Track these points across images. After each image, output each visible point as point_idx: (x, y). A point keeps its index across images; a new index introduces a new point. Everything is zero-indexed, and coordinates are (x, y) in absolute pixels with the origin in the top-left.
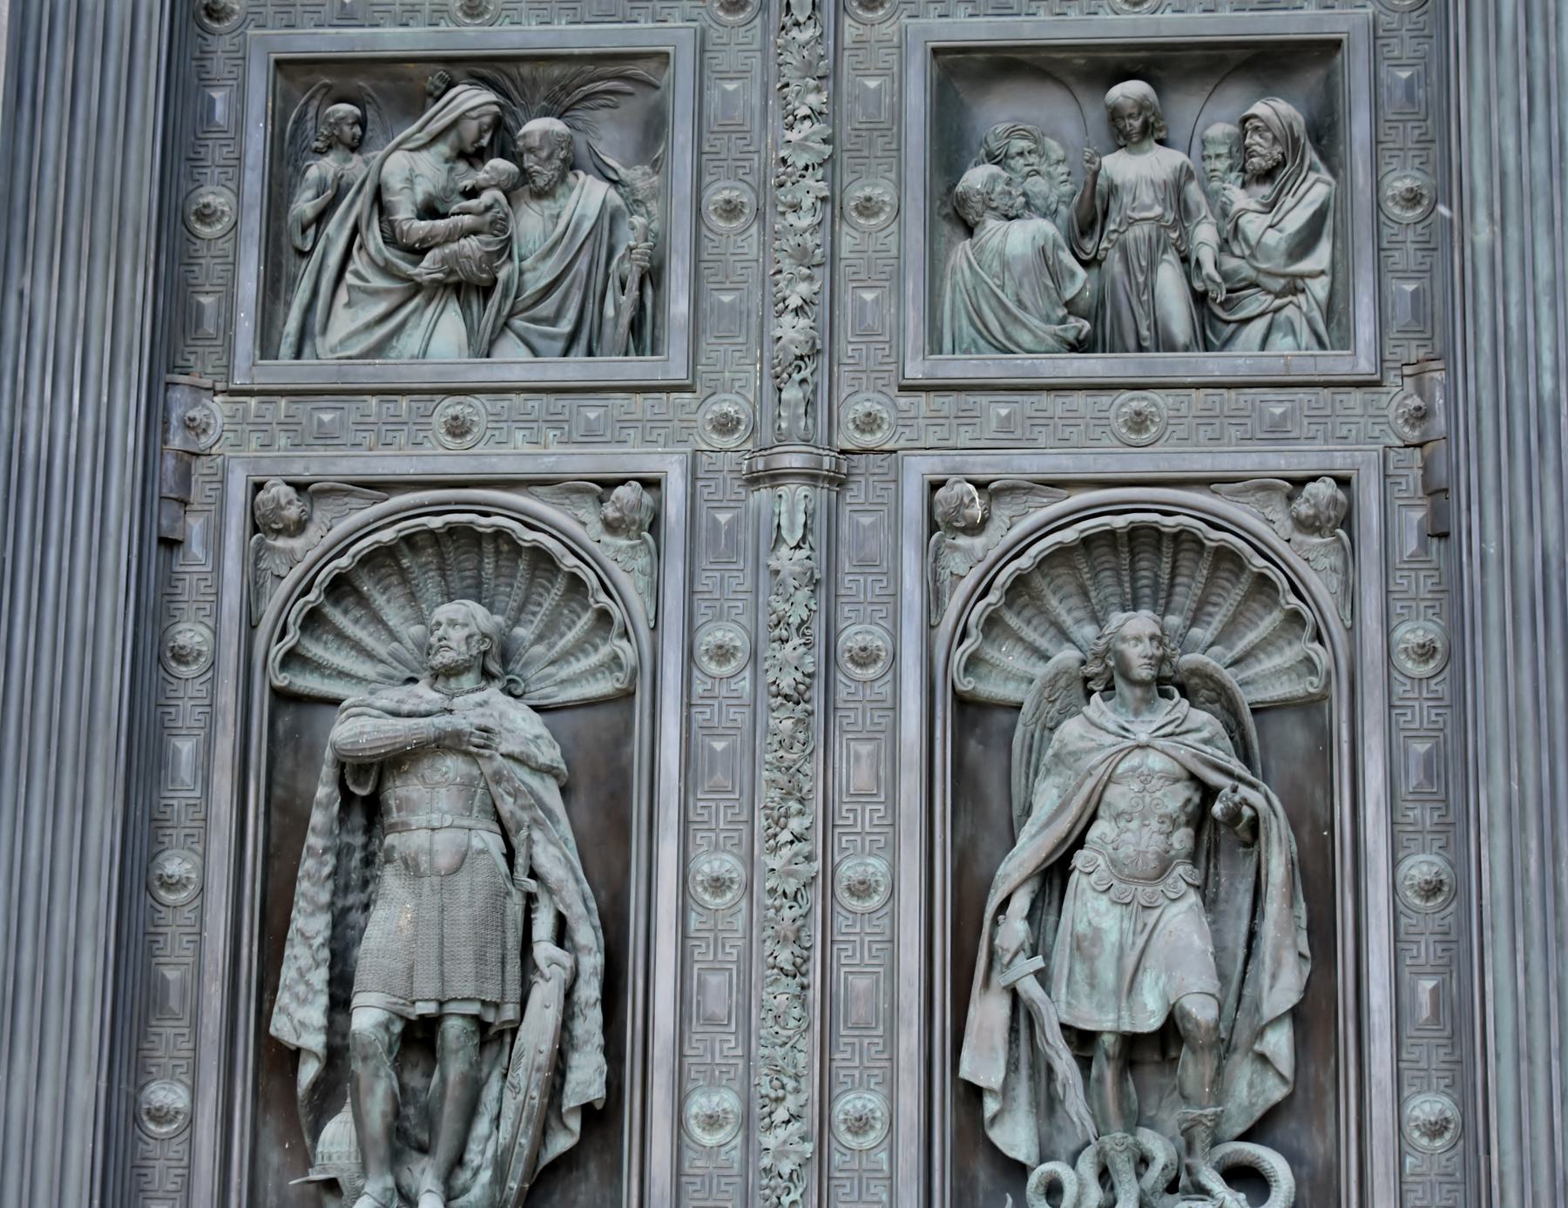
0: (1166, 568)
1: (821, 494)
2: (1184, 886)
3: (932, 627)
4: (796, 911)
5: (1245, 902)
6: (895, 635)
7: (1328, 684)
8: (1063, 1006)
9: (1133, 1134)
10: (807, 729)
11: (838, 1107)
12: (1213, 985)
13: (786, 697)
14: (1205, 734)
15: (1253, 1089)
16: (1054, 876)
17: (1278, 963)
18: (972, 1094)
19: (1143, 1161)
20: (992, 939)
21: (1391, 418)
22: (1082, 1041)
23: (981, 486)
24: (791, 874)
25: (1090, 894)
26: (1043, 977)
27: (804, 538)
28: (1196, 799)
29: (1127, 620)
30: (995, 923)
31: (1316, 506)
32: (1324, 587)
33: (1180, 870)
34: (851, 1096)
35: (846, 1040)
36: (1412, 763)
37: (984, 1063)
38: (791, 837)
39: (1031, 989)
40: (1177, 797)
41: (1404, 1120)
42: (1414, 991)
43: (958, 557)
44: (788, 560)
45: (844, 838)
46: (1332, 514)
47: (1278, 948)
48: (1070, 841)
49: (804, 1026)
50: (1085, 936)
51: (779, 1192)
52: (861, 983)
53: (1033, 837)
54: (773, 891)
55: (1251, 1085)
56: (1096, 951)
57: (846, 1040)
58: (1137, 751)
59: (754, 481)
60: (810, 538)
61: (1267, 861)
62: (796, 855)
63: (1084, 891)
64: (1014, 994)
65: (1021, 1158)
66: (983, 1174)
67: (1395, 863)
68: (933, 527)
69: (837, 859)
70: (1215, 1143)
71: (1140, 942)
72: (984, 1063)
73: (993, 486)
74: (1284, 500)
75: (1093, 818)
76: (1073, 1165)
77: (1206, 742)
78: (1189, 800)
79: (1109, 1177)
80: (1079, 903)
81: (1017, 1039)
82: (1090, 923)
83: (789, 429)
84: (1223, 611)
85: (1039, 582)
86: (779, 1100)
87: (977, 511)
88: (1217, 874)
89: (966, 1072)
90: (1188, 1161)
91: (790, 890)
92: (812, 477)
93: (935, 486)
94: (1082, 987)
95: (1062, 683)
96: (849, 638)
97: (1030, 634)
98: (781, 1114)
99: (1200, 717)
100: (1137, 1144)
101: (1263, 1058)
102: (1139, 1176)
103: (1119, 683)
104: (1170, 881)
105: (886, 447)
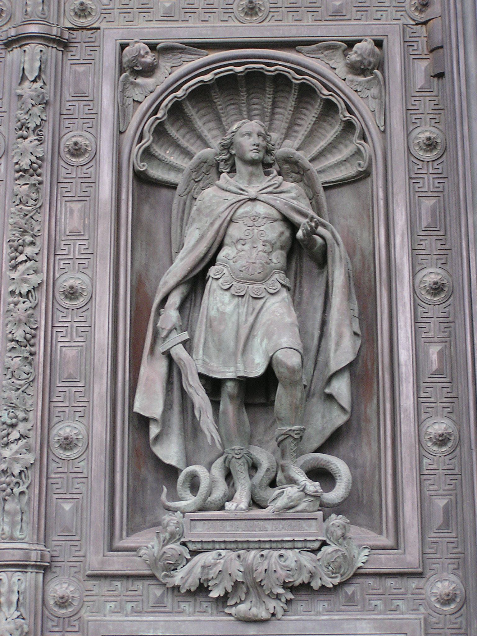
0: (269, 102)
1: (52, 53)
2: (279, 286)
3: (121, 133)
4: (28, 305)
5: (319, 302)
6: (97, 138)
7: (370, 165)
8: (200, 362)
9: (248, 448)
10: (38, 191)
11: (54, 432)
12: (297, 343)
13: (25, 171)
14: (293, 194)
15: (325, 420)
16: (196, 283)
17: (340, 336)
18: (142, 423)
19: (254, 467)
20: (155, 322)
21: (407, 7)
22: (213, 386)
23: (153, 47)
24: (25, 281)
25: (219, 292)
26: (188, 344)
27: (39, 77)
28: (287, 234)
29: (244, 123)
30: (158, 314)
31: (360, 55)
32: (366, 108)
33: (277, 276)
34: (61, 425)
35: (60, 389)
36: (423, 212)
37: (150, 401)
38: (25, 258)
39: (179, 352)
40: (275, 231)
41: (422, 435)
42: (427, 354)
43: (137, 91)
44: (28, 89)
45: (62, 262)
46: (372, 60)
47: (339, 326)
48: (207, 260)
49: (31, 379)
50: (215, 317)
51: (12, 486)
52: (70, 353)
53: (182, 259)
54: (12, 293)
55: (323, 417)
56: (222, 327)
57: (60, 389)
58: (249, 202)
59: (9, 44)
60: (43, 76)
61: (333, 272)
62: (28, 269)
63: (215, 290)
64: (168, 355)
65: (173, 462)
66: (149, 474)
67: (414, 274)
68: (122, 70)
69: (57, 275)
70: (300, 453)
71: (251, 319)
72: (150, 401)
73: (159, 46)
74: (342, 56)
75: (221, 246)
76: (209, 470)
77: (293, 198)
78: (282, 233)
79: (232, 478)
80: (211, 299)
81: (172, 388)
82: (218, 309)
83: (32, 12)
84: (305, 128)
85: (190, 110)
86: (13, 426)
87: (149, 59)
88: (301, 287)
89: (137, 408)
90: (282, 462)
91: (24, 291)
92: (46, 39)
93: (123, 47)
94: (213, 350)
95: (204, 170)
96: (68, 140)
97: (184, 142)
98: (15, 435)
99: (288, 185)
100: (249, 454)
101: (330, 397)
102: (251, 477)
103: (239, 165)
104: (270, 282)
105: (95, 26)
